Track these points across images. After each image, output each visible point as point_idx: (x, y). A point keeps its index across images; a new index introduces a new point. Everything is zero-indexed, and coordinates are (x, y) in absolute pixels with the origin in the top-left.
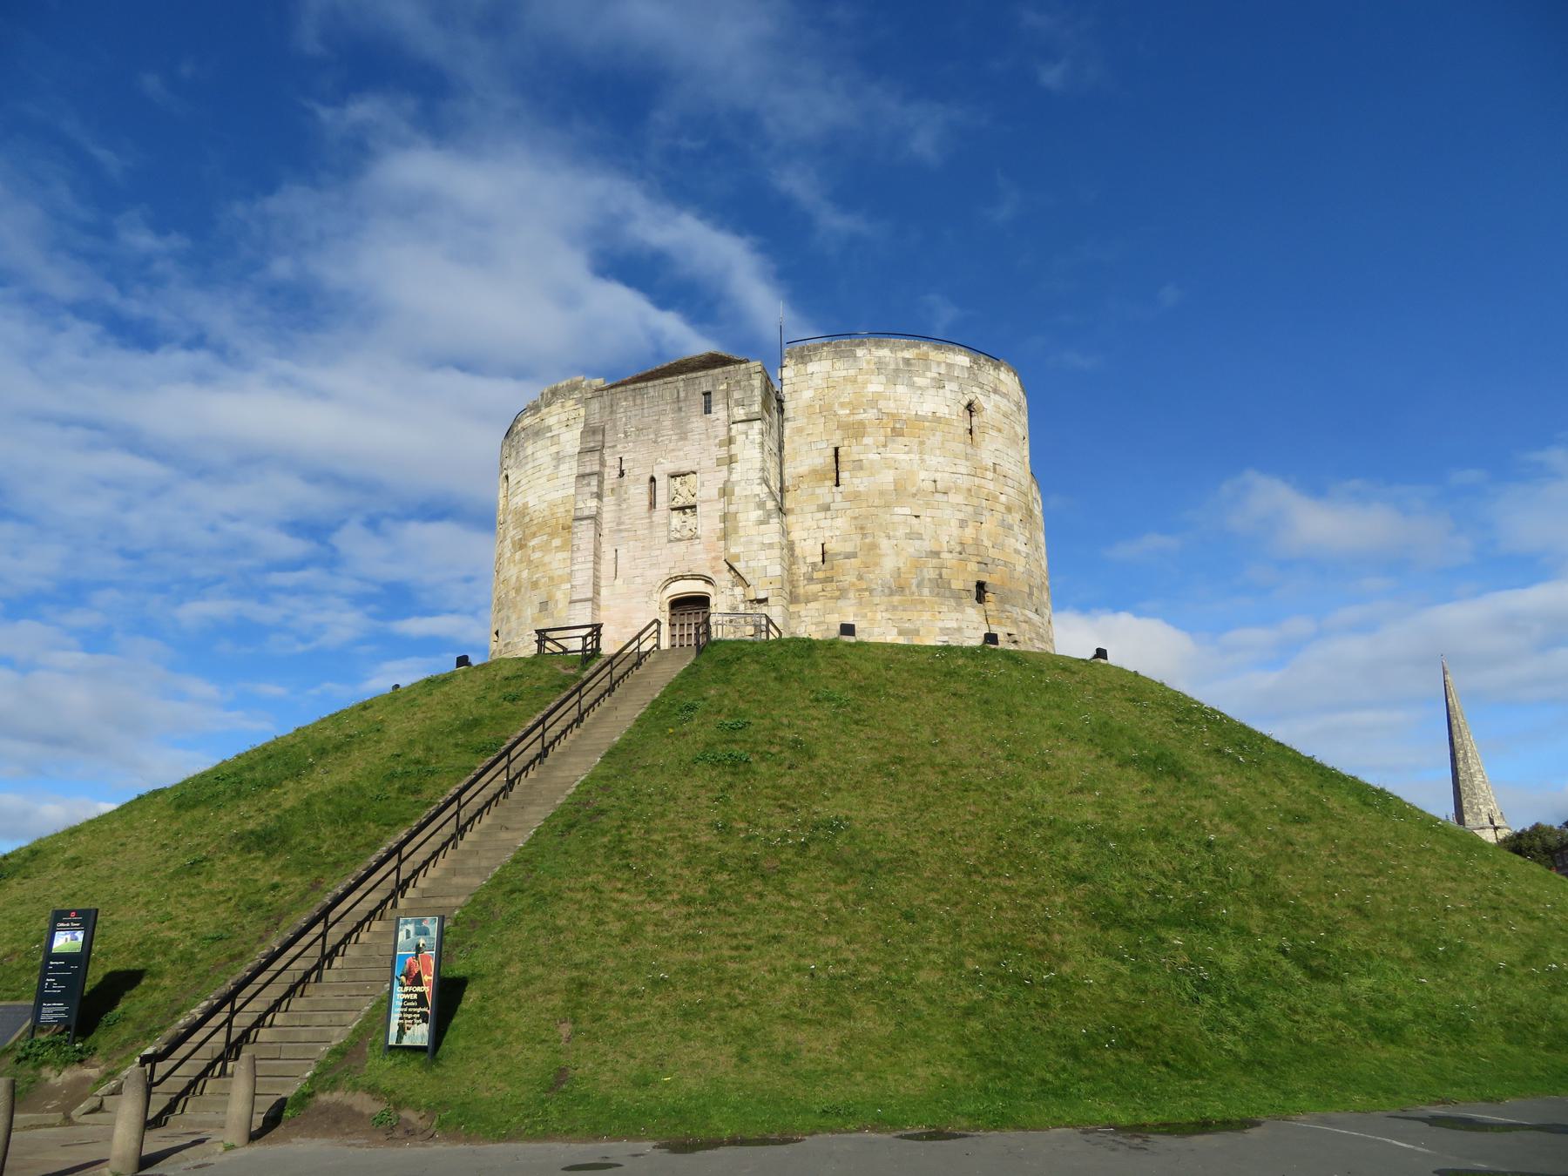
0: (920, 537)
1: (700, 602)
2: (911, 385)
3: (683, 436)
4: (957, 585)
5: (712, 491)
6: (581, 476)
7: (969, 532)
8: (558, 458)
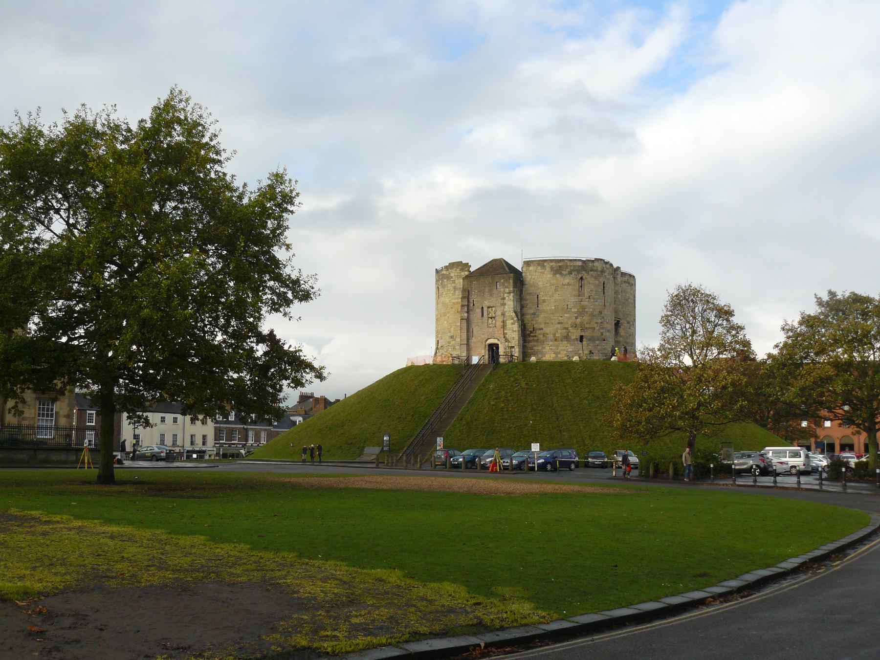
0: (561, 323)
1: (497, 346)
2: (561, 274)
3: (491, 295)
4: (573, 337)
5: (499, 313)
6: (462, 306)
7: (579, 320)
8: (455, 288)
